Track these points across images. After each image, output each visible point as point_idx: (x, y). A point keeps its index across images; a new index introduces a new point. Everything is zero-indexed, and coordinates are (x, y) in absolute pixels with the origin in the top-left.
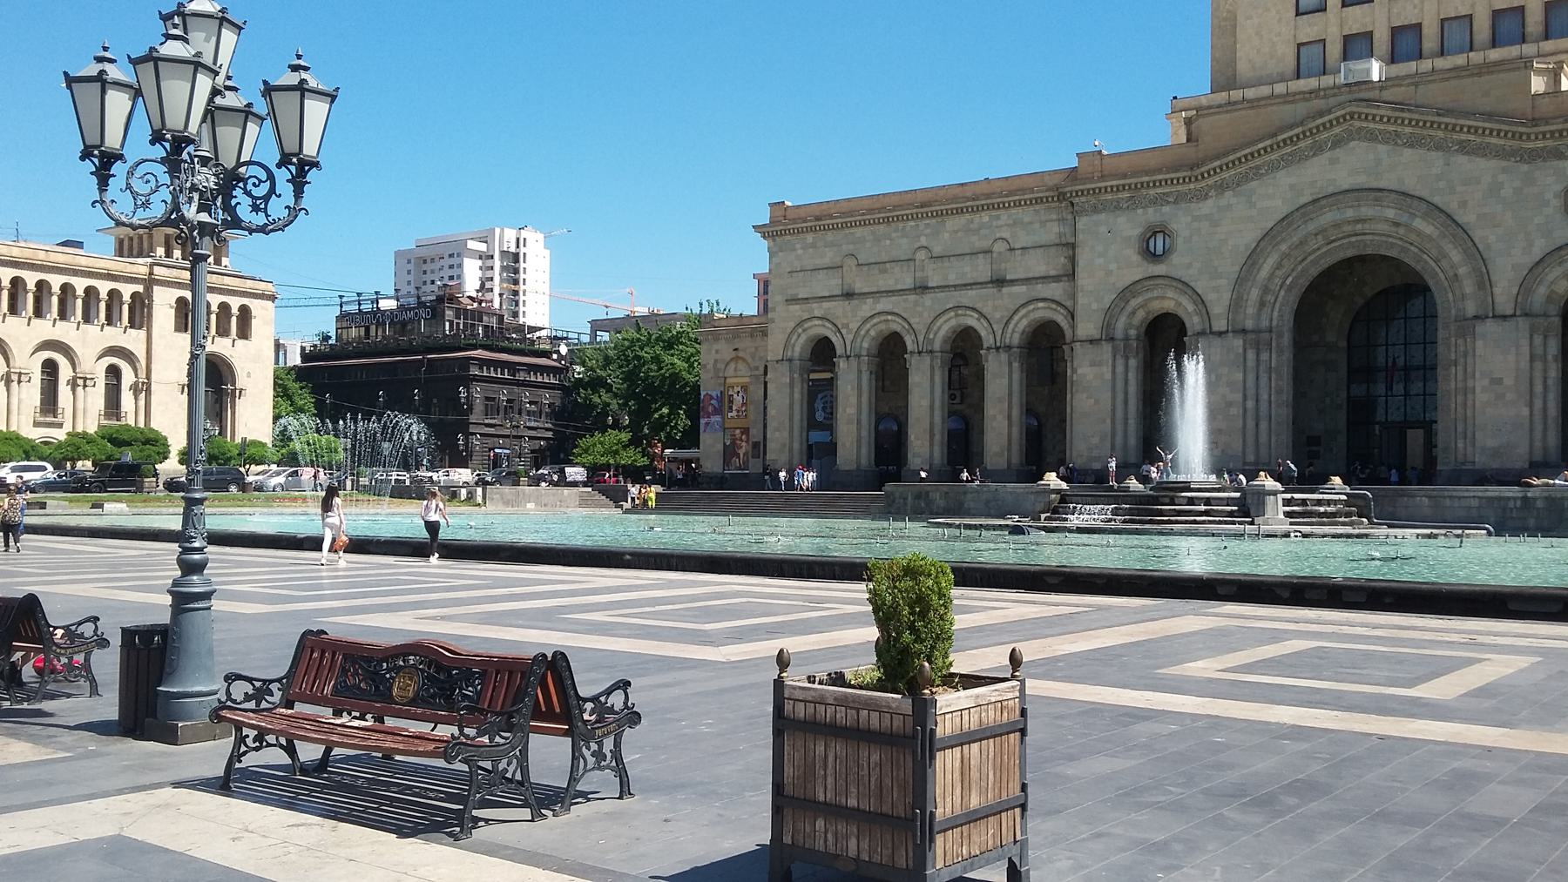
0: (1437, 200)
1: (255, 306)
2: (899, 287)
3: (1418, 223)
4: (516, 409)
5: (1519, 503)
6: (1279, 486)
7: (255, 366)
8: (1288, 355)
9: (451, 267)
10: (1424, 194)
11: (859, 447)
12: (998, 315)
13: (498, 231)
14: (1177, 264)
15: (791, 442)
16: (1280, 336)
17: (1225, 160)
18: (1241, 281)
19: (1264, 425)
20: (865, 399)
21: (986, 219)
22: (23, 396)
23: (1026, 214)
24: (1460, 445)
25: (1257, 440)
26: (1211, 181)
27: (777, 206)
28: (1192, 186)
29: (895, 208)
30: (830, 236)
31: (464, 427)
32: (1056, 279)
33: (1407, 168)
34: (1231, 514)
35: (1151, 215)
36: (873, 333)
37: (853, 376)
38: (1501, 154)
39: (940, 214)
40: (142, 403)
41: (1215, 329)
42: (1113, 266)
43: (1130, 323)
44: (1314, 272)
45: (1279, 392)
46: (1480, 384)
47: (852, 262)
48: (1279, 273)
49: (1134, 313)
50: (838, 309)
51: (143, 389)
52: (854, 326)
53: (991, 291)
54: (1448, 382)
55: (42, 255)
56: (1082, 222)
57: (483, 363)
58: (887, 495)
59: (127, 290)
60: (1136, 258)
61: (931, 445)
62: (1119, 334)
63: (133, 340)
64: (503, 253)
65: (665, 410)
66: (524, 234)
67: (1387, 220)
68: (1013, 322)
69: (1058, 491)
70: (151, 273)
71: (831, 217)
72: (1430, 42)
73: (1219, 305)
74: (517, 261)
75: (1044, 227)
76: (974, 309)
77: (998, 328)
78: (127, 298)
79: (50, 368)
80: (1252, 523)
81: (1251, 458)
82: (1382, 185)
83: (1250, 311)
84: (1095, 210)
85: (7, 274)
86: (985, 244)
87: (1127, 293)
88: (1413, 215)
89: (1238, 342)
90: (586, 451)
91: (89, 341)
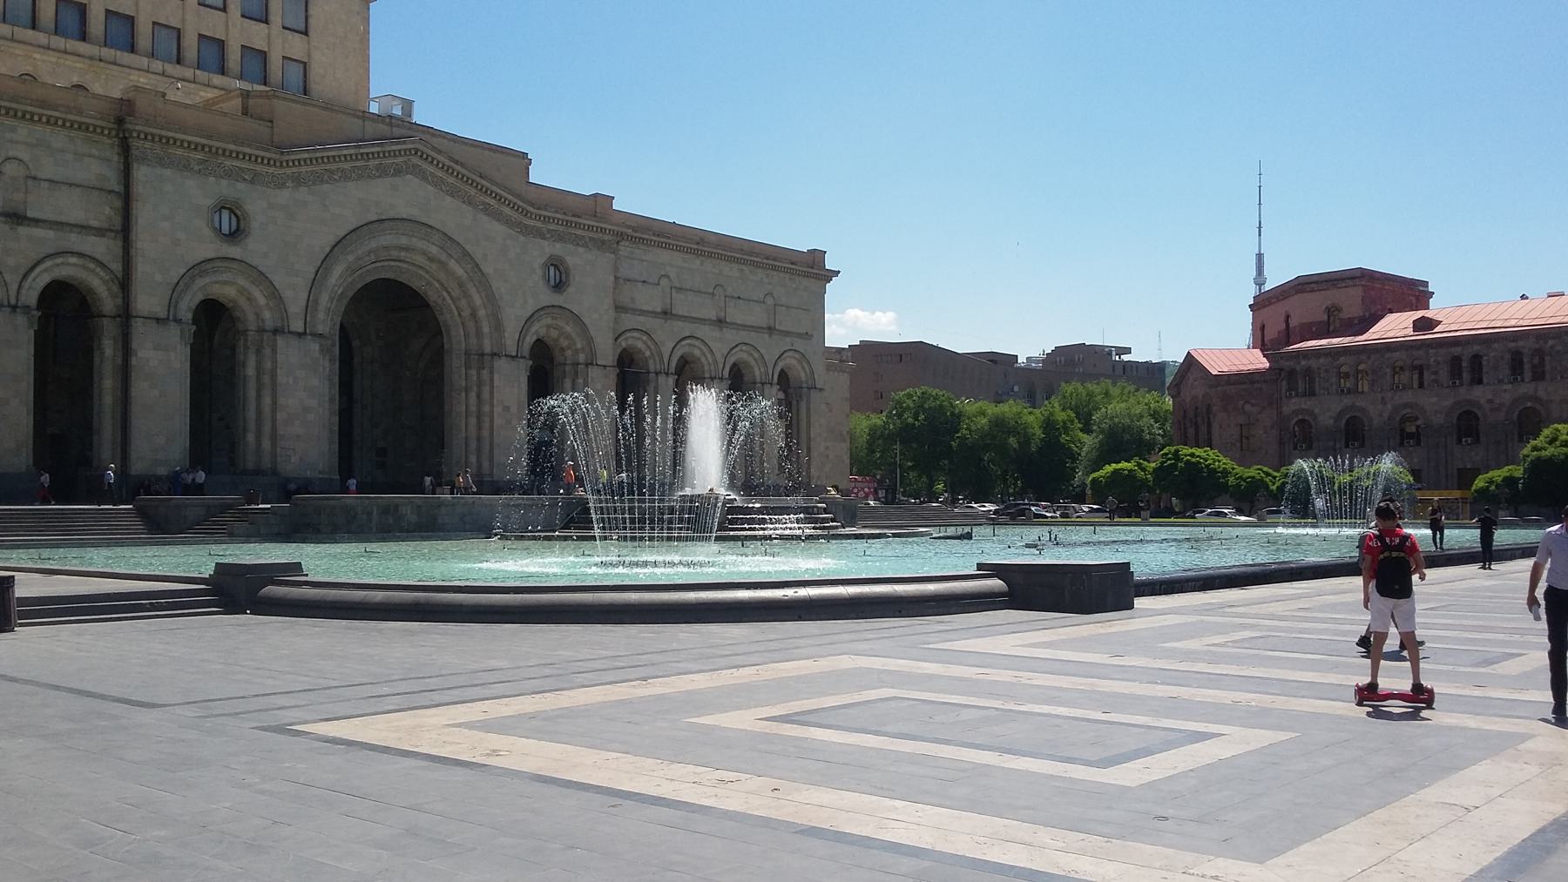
0: (468, 248)
3: (453, 264)
10: (460, 239)
12: (11, 261)
14: (253, 249)
18: (316, 282)
23: (58, 139)
24: (473, 459)
26: (289, 171)
28: (271, 170)
32: (100, 232)
33: (449, 214)
38: (508, 222)
46: (498, 410)
54: (460, 408)
60: (207, 232)
67: (424, 253)
72: (144, 41)
73: (296, 306)
84: (161, 162)
87: (200, 268)
89: (315, 347)
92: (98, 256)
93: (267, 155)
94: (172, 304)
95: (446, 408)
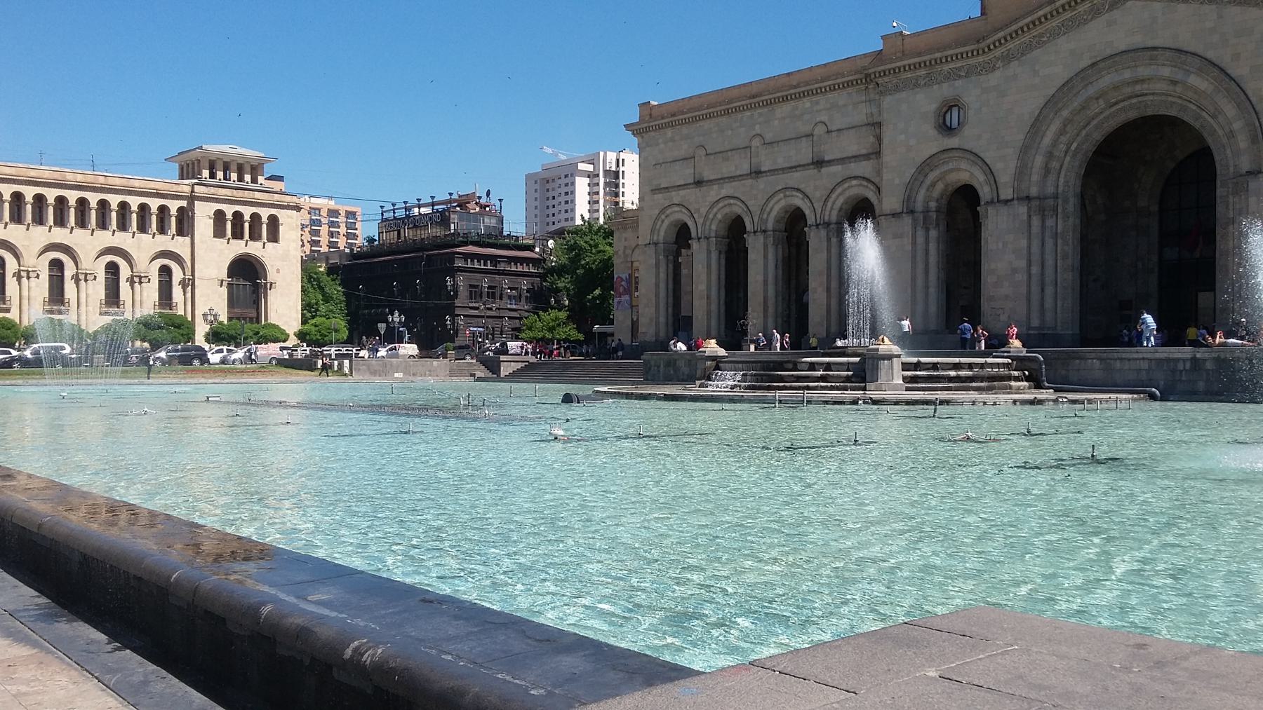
0: (1210, 55)
1: (282, 215)
2: (738, 173)
3: (1194, 80)
4: (498, 295)
5: (1188, 365)
6: (896, 349)
7: (284, 264)
8: (1073, 221)
9: (567, 185)
10: (1200, 51)
11: (709, 319)
12: (818, 194)
13: (602, 154)
14: (969, 137)
15: (658, 318)
16: (1066, 201)
17: (1008, 30)
19: (1049, 290)
20: (714, 277)
21: (808, 105)
22: (90, 291)
23: (840, 97)
25: (1042, 305)
26: (998, 53)
27: (645, 106)
28: (981, 59)
29: (730, 102)
30: (685, 130)
31: (451, 310)
32: (866, 157)
34: (848, 379)
35: (945, 91)
36: (719, 216)
37: (703, 256)
39: (769, 103)
40: (189, 295)
41: (1002, 197)
42: (912, 142)
43: (929, 196)
44: (1098, 136)
45: (1065, 257)
47: (702, 152)
48: (1064, 139)
49: (933, 185)
50: (691, 195)
51: (189, 284)
52: (704, 211)
53: (812, 172)
55: (102, 180)
56: (888, 101)
57: (467, 256)
58: (646, 363)
59: (173, 206)
60: (933, 132)
61: (765, 317)
62: (919, 206)
63: (180, 245)
64: (607, 172)
65: (597, 292)
66: (623, 156)
68: (831, 200)
69: (714, 358)
70: (193, 191)
71: (683, 113)
74: (617, 177)
75: (848, 109)
76: (798, 190)
77: (818, 206)
78: (174, 211)
79: (113, 269)
80: (864, 389)
81: (1035, 322)
82: (1157, 43)
83: (1035, 178)
84: (897, 89)
85: (7, 190)
86: (806, 129)
88: (1188, 72)
89: (1022, 210)
90: (530, 329)
91: (143, 247)
92: (867, 175)
93: (968, 48)
94: (909, 200)
95: (1220, 245)
